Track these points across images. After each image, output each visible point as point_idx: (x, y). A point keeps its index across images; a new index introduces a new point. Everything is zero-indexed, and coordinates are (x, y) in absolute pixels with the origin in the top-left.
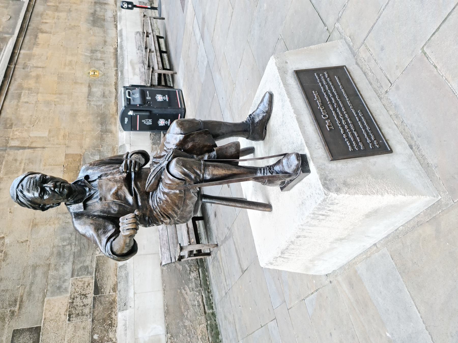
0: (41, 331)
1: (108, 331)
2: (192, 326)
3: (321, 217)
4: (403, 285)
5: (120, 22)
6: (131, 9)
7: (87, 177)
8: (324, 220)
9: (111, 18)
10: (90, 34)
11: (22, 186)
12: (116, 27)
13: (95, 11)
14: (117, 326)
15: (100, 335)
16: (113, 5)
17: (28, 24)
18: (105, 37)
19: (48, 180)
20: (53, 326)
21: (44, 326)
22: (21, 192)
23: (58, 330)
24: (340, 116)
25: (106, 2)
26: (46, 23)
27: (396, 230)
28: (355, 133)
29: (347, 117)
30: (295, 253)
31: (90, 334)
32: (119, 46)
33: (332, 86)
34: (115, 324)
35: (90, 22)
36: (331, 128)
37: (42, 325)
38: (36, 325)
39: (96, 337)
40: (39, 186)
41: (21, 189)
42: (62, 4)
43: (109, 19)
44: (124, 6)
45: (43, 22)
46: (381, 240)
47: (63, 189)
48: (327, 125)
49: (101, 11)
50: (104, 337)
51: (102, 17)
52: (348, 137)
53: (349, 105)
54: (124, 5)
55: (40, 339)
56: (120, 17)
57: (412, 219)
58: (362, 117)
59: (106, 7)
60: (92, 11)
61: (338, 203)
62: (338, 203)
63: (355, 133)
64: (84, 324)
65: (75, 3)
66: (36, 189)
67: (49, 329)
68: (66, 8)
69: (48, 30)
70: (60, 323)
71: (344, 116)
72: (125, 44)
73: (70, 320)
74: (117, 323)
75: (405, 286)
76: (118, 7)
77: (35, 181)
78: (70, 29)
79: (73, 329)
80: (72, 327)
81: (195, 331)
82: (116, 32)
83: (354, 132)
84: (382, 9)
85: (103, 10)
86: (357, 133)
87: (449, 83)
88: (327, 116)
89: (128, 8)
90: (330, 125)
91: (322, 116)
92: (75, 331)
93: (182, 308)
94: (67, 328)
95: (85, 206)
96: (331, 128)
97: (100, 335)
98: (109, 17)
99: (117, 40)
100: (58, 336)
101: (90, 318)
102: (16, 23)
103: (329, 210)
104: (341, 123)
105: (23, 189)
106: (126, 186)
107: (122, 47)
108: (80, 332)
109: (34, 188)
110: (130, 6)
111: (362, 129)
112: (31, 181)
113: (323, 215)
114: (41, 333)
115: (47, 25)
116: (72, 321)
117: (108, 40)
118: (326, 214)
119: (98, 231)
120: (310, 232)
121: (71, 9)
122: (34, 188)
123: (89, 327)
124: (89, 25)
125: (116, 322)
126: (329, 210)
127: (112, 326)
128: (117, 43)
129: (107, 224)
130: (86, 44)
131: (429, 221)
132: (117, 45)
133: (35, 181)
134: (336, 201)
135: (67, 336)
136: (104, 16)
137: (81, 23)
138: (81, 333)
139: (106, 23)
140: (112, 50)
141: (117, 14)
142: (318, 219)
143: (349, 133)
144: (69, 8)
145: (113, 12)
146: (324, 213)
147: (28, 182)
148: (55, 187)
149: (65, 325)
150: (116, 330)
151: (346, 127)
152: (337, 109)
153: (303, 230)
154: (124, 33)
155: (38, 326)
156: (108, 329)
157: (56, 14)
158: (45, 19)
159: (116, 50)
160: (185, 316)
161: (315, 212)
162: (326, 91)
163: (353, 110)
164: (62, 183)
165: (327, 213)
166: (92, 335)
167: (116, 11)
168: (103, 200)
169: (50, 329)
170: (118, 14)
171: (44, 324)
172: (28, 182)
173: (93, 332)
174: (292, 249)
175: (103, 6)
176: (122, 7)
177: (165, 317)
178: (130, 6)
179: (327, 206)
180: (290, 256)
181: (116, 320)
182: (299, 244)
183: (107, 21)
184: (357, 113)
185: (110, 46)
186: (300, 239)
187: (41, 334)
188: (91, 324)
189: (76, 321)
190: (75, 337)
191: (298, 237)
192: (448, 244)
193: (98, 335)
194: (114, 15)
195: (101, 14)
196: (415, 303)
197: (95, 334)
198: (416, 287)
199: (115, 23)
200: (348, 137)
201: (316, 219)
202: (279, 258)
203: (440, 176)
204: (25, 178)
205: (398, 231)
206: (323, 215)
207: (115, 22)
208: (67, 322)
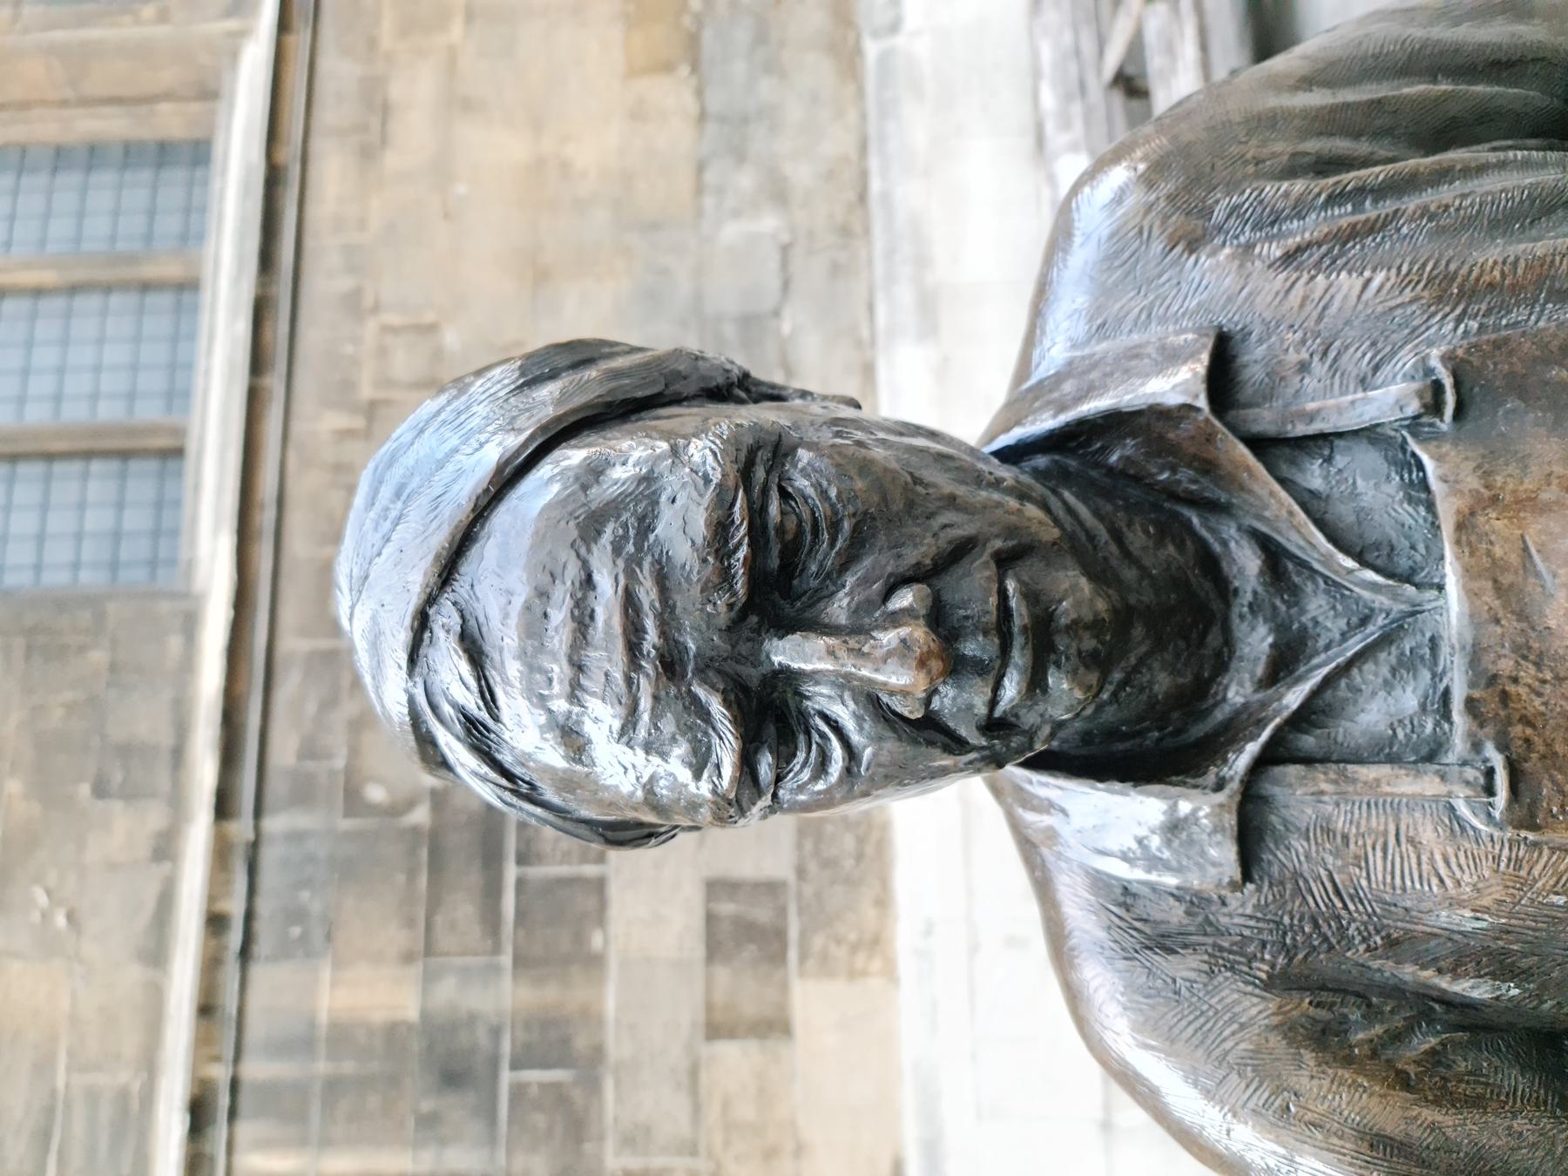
11: (474, 649)
19: (826, 554)
22: (478, 735)
40: (705, 668)
41: (472, 703)
47: (1036, 684)
66: (686, 729)
105: (488, 697)
109: (645, 703)
112: (588, 582)
122: (645, 703)
133: (647, 594)
147: (543, 594)
164: (1005, 561)
172: (543, 594)
204: (502, 517)
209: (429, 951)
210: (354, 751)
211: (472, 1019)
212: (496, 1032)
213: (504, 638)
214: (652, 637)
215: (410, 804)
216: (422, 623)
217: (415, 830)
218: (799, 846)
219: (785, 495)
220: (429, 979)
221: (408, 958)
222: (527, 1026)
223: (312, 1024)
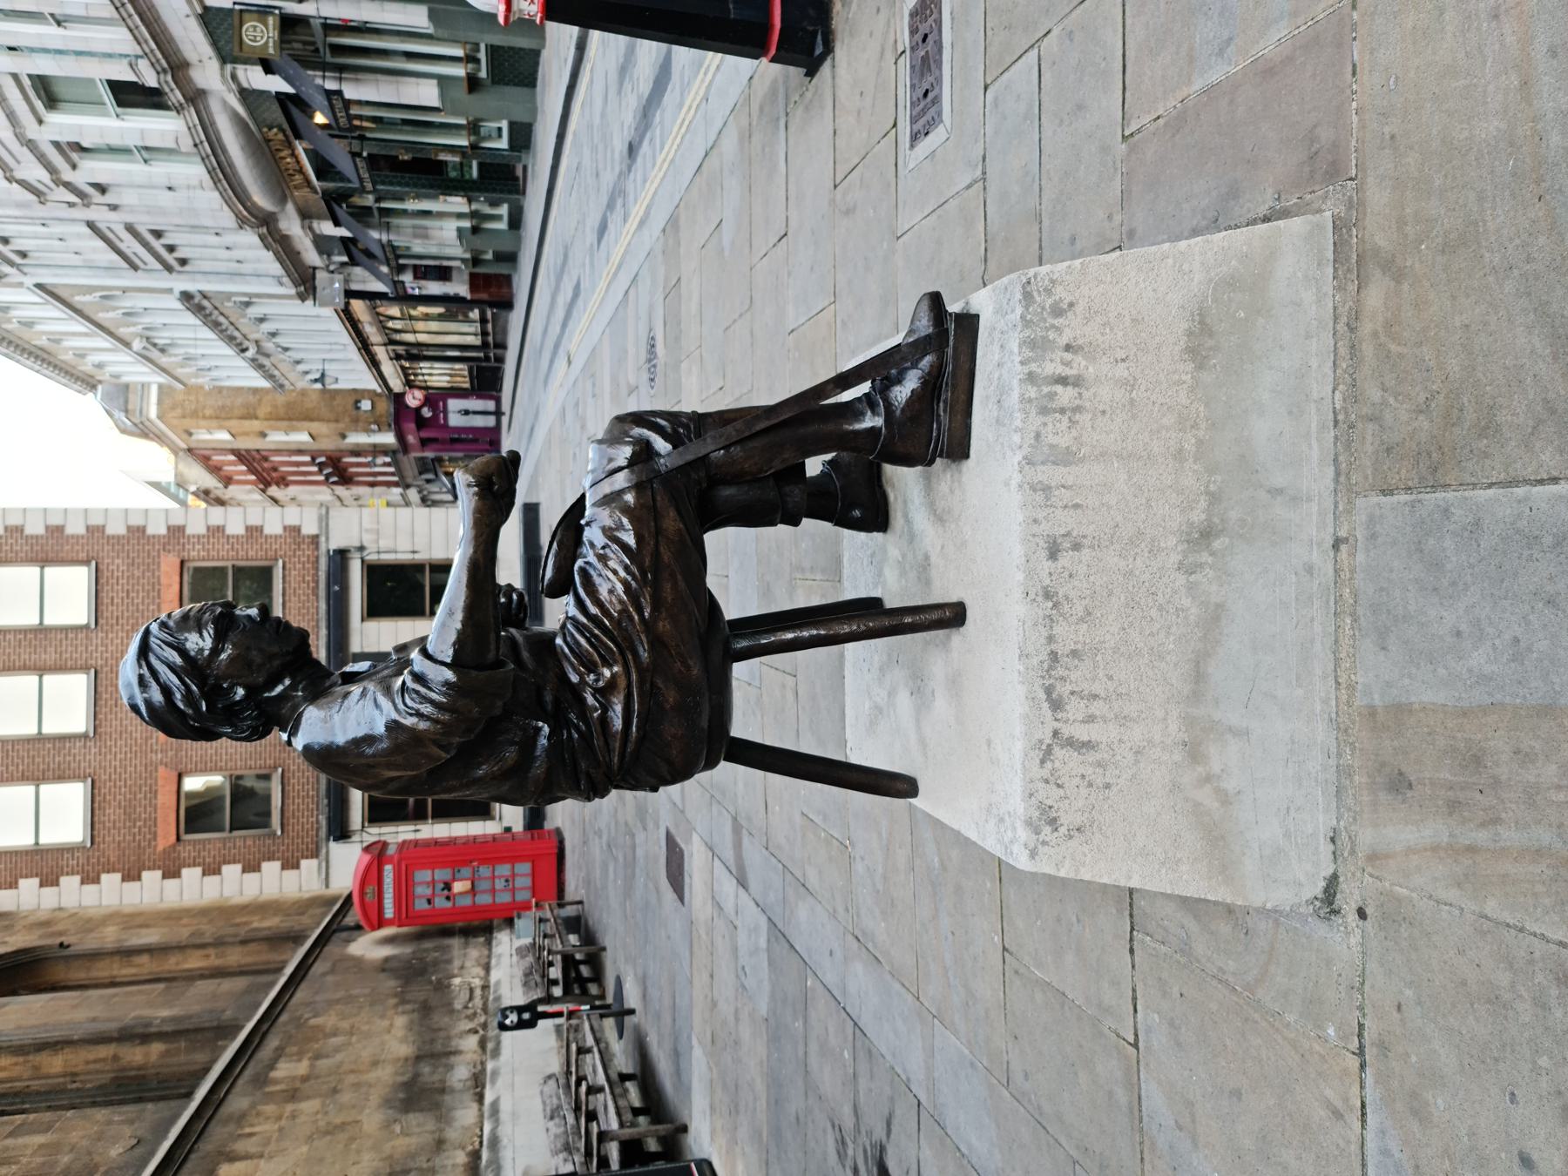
3: (1066, 395)
4: (1466, 499)
5: (493, 1082)
6: (530, 1024)
8: (1078, 409)
9: (466, 1080)
10: (393, 1132)
12: (480, 1098)
13: (416, 1076)
16: (475, 1052)
17: (192, 1146)
18: (441, 1130)
25: (453, 1049)
26: (251, 1135)
27: (1336, 422)
30: (1097, 688)
32: (485, 1143)
35: (397, 1104)
42: (313, 1081)
43: (459, 1086)
44: (508, 1022)
45: (240, 1136)
46: (1336, 507)
49: (434, 1072)
51: (437, 1085)
54: (507, 1017)
56: (495, 1073)
57: (1336, 344)
59: (453, 1059)
60: (401, 1079)
61: (1071, 305)
62: (1071, 305)
65: (352, 1071)
68: (325, 1087)
69: (253, 1150)
72: (505, 1132)
75: (1471, 493)
76: (488, 1053)
78: (327, 1133)
82: (480, 1110)
84: (1038, 204)
85: (441, 1069)
87: (1190, 95)
89: (521, 1025)
98: (460, 1081)
99: (482, 1130)
102: (152, 1154)
103: (1068, 348)
107: (495, 1142)
110: (526, 1016)
113: (1063, 381)
115: (254, 1139)
117: (452, 1134)
118: (1068, 372)
120: (1077, 506)
121: (339, 1087)
124: (390, 1112)
126: (1068, 348)
128: (481, 1137)
130: (374, 1160)
131: (1359, 284)
132: (481, 1143)
134: (1059, 292)
136: (443, 1081)
137: (367, 1111)
139: (447, 1098)
140: (461, 1158)
141: (484, 1070)
142: (1062, 411)
144: (334, 1085)
145: (474, 1067)
146: (1060, 370)
153: (1047, 489)
154: (505, 1107)
157: (289, 1108)
158: (252, 1125)
159: (476, 1155)
161: (1033, 367)
165: (1067, 364)
167: (483, 1063)
170: (490, 1066)
174: (1074, 653)
175: (444, 1060)
176: (503, 1027)
178: (526, 1016)
179: (1053, 326)
180: (1090, 719)
182: (1079, 609)
183: (453, 1091)
185: (455, 1149)
186: (1065, 559)
191: (1053, 554)
192: (1423, 247)
194: (474, 1074)
195: (436, 1077)
196: (1527, 482)
198: (1485, 441)
199: (478, 1090)
201: (1055, 411)
202: (1058, 752)
203: (1298, 196)
205: (1341, 417)
206: (1063, 381)
207: (477, 1087)
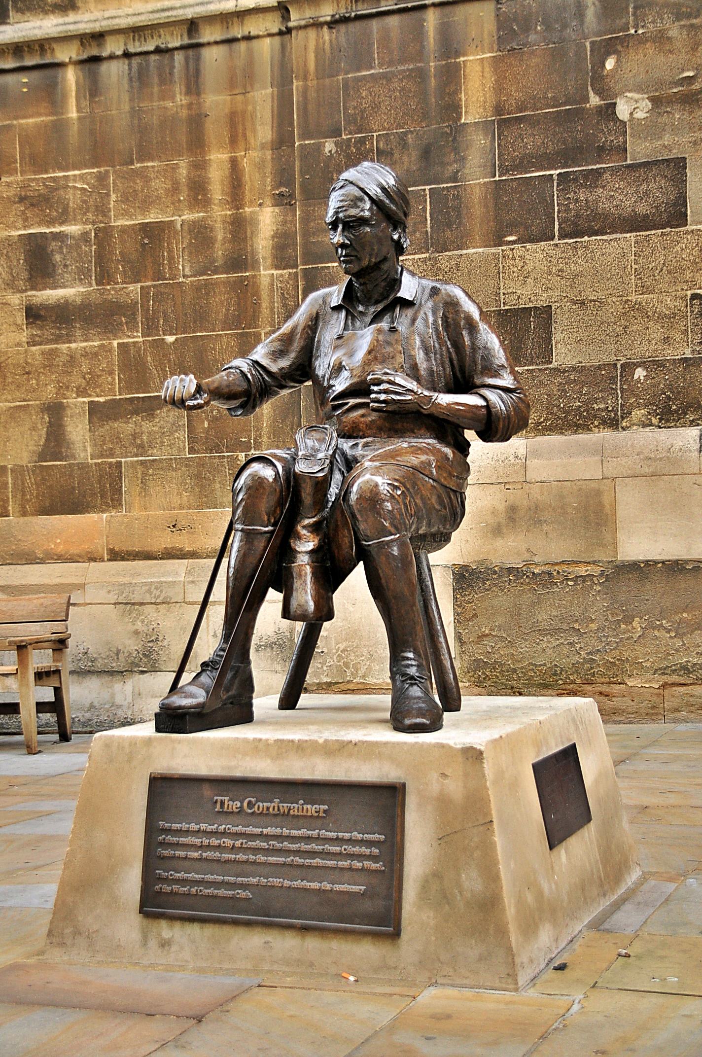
0: (673, 230)
1: (651, 404)
2: (628, 639)
7: (407, 304)
14: (660, 428)
15: (642, 384)
20: (684, 256)
21: (687, 233)
23: (669, 272)
24: (244, 841)
28: (196, 855)
29: (238, 856)
31: (650, 357)
33: (335, 862)
34: (668, 421)
36: (218, 805)
37: (689, 228)
38: (691, 212)
39: (640, 373)
48: (227, 798)
50: (637, 396)
52: (188, 832)
53: (270, 879)
55: (653, 232)
58: (233, 892)
63: (196, 855)
64: (678, 337)
67: (678, 248)
70: (688, 275)
71: (241, 849)
73: (694, 300)
74: (669, 427)
77: (344, 209)
79: (667, 312)
80: (675, 306)
81: (615, 645)
83: (200, 852)
86: (193, 859)
88: (250, 811)
90: (226, 806)
91: (253, 800)
92: (661, 317)
93: (685, 615)
94: (673, 294)
95: (338, 309)
96: (218, 805)
97: (642, 384)
100: (654, 276)
101: (693, 351)
104: (224, 834)
106: (351, 385)
108: (656, 332)
111: (203, 876)
114: (668, 229)
116: (691, 306)
119: (279, 340)
123: (671, 353)
125: (673, 424)
127: (662, 414)
129: (293, 355)
133: (344, 209)
135: (652, 299)
138: (655, 335)
143: (200, 840)
148: (343, 246)
149: (682, 289)
150: (651, 425)
151: (215, 842)
152: (265, 844)
155: (688, 217)
156: (657, 406)
160: (658, 623)
162: (318, 839)
163: (255, 880)
166: (645, 362)
168: (340, 341)
169: (674, 250)
171: (692, 231)
173: (654, 365)
177: (663, 562)
181: (678, 424)
184: (244, 886)
187: (664, 230)
188: (677, 357)
189: (689, 314)
190: (646, 319)
193: (642, 378)
197: (647, 371)
200: (188, 832)
208: (689, 293)
209: (503, 123)
210: (642, 40)
211: (463, 159)
212: (454, 179)
213: (342, 191)
214: (340, 210)
215: (599, 93)
216: (346, 180)
217: (586, 99)
218: (574, 369)
219: (360, 226)
220: (486, 125)
221: (499, 109)
222: (458, 197)
223: (458, 54)
